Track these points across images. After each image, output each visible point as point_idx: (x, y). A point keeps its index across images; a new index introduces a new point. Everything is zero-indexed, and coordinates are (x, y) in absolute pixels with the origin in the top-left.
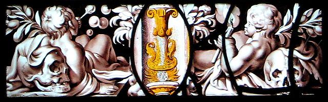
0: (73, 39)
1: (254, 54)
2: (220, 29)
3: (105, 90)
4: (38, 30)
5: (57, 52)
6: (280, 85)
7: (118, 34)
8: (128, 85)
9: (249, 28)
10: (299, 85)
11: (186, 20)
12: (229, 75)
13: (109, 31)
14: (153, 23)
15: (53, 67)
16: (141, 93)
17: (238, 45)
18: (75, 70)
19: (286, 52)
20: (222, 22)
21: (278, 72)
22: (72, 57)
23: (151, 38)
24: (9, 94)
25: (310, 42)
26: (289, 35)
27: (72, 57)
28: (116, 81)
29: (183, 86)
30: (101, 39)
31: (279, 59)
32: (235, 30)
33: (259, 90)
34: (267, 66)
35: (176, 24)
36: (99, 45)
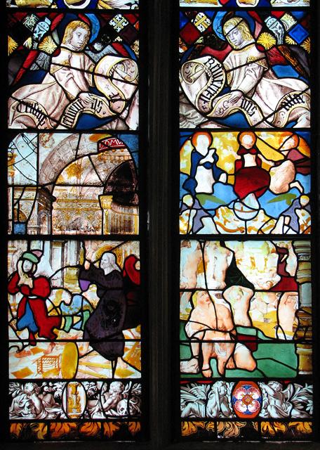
0: (37, 396)
1: (113, 401)
2: (99, 392)
3: (50, 417)
4: (22, 392)
5: (30, 401)
6: (124, 414)
7: (56, 394)
8: (60, 414)
9: (111, 391)
10: (132, 414)
11: (84, 388)
12: (102, 410)
13: (53, 393)
14: (71, 389)
15: (28, 407)
16: (65, 418)
17: (106, 398)
18: (38, 408)
19: (126, 401)
20: (99, 389)
21: (123, 409)
22: (37, 403)
23: (70, 395)
24: (10, 418)
25: (136, 397)
26: (127, 394)
27: (37, 403)
28: (55, 413)
29: (83, 415)
30: (49, 396)
31: (123, 404)
32: (105, 392)
33: (115, 416)
34: (118, 407)
35: (80, 389)
36: (48, 398)
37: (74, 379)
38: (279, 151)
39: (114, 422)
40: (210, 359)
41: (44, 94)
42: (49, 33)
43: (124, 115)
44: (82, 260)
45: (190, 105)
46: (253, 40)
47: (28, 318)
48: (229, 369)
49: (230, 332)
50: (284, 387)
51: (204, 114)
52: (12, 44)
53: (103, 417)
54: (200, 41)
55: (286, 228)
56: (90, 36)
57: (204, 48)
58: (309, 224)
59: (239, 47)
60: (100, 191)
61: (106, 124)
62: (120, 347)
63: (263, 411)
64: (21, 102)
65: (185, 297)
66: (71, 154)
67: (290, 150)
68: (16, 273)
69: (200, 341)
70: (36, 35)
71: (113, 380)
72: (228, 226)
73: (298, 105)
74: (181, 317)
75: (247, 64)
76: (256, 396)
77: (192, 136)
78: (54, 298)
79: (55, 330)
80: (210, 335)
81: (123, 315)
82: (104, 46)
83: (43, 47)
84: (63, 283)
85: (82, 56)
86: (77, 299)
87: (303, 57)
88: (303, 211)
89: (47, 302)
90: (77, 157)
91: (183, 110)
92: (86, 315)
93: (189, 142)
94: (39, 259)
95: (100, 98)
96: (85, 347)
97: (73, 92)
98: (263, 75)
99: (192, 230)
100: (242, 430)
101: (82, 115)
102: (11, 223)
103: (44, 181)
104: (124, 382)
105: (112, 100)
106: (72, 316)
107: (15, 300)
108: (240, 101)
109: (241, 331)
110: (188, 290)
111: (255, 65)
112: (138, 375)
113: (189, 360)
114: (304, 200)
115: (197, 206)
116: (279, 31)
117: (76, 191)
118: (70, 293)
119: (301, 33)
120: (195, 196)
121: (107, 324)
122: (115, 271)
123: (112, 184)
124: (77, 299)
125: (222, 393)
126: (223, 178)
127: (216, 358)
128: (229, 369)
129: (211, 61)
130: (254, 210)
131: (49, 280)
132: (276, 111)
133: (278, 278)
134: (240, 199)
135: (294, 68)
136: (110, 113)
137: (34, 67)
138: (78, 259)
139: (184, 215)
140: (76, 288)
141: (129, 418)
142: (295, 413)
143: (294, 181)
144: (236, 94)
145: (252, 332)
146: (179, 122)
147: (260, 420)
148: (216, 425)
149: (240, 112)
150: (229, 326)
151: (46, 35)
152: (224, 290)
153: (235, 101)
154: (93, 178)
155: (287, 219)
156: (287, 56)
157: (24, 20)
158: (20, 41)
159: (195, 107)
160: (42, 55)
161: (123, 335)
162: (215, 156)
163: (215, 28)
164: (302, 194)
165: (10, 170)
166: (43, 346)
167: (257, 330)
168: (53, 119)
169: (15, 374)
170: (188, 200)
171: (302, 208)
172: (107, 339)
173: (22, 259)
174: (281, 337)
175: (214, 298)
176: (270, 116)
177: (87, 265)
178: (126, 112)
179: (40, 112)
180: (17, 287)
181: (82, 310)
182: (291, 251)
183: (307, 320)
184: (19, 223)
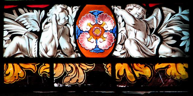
50: (149, 13)
63: (119, 47)
76: (109, 25)
100: (89, 75)
125: (62, 22)
142: (165, 51)
147: (114, 60)
148: (52, 69)
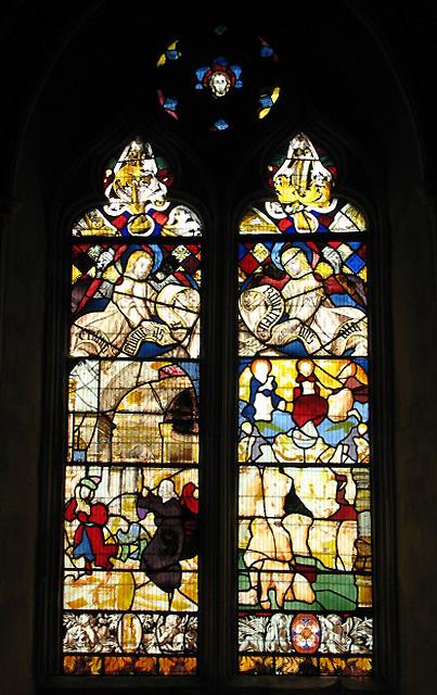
2: (155, 625)
3: (105, 650)
4: (77, 623)
5: (85, 633)
7: (111, 626)
9: (167, 625)
13: (108, 625)
31: (179, 638)
33: (171, 651)
35: (136, 621)
37: (130, 611)
38: (337, 379)
39: (170, 657)
40: (269, 589)
41: (106, 322)
42: (112, 263)
43: (186, 343)
44: (140, 487)
45: (250, 333)
46: (311, 270)
47: (84, 547)
48: (288, 601)
49: (289, 562)
50: (344, 621)
51: (262, 342)
52: (76, 273)
53: (159, 652)
54: (259, 270)
55: (345, 457)
56: (153, 266)
57: (263, 277)
58: (368, 453)
59: (298, 276)
60: (160, 419)
61: (167, 352)
62: (176, 579)
63: (322, 645)
64: (84, 330)
65: (243, 527)
66: (132, 382)
67: (348, 378)
68: (73, 499)
69: (259, 571)
70: (100, 265)
71: (170, 612)
72: (287, 454)
73: (355, 333)
74: (240, 546)
75: (305, 293)
76: (315, 629)
77: (251, 363)
78: (112, 527)
79: (111, 559)
80: (269, 565)
81: (181, 546)
82: (167, 275)
83: (105, 276)
84: (120, 511)
85: (144, 284)
86: (135, 527)
87: (361, 286)
88: (361, 440)
89: (105, 530)
90: (138, 385)
91: (242, 338)
92: (143, 545)
93: (248, 369)
94: (97, 485)
95: (161, 327)
96: (141, 577)
97: (135, 320)
98: (321, 303)
99: (250, 458)
100: (301, 665)
101: (143, 342)
102: (70, 450)
103: (104, 408)
104: (181, 615)
105: (173, 328)
106: (129, 545)
107: (71, 527)
108: (299, 329)
109: (300, 561)
110: (247, 518)
111: (313, 294)
112: (196, 609)
113: (246, 591)
114: (363, 429)
115: (256, 433)
116: (337, 261)
117: (136, 419)
118: (128, 521)
119: (358, 261)
120: (253, 423)
121: (163, 554)
122: (173, 499)
123: (172, 411)
124: (135, 527)
125: (281, 626)
126: (281, 405)
127: (275, 589)
128: (288, 601)
129: (270, 290)
130: (313, 438)
131: (106, 507)
132: (334, 339)
133: (336, 507)
134: (298, 426)
135: (351, 296)
136: (171, 341)
137: (97, 296)
138: (136, 486)
139: (243, 444)
140: (133, 516)
141: (187, 653)
142: (355, 649)
143: (352, 409)
144: (296, 322)
145: (310, 562)
146: (238, 349)
147: (318, 655)
148: (274, 661)
149: (298, 340)
150: (288, 557)
151: (109, 265)
152: (282, 518)
153: (293, 329)
154: (154, 406)
155: (346, 448)
156: (345, 285)
157: (88, 251)
158: (84, 270)
159: (254, 335)
160: (105, 284)
161: (180, 566)
162: (274, 384)
163: (273, 257)
164: (360, 422)
165: (71, 397)
166: (100, 575)
167: (316, 559)
168: (115, 347)
169: (69, 603)
170: (247, 427)
171: (361, 436)
172: (164, 569)
173: (80, 485)
174: (340, 567)
175: (273, 526)
176: (328, 344)
177: (145, 492)
178: (187, 340)
179: (103, 340)
180: (74, 513)
181: (139, 539)
182: (350, 478)
183: (367, 551)
184: (78, 450)
